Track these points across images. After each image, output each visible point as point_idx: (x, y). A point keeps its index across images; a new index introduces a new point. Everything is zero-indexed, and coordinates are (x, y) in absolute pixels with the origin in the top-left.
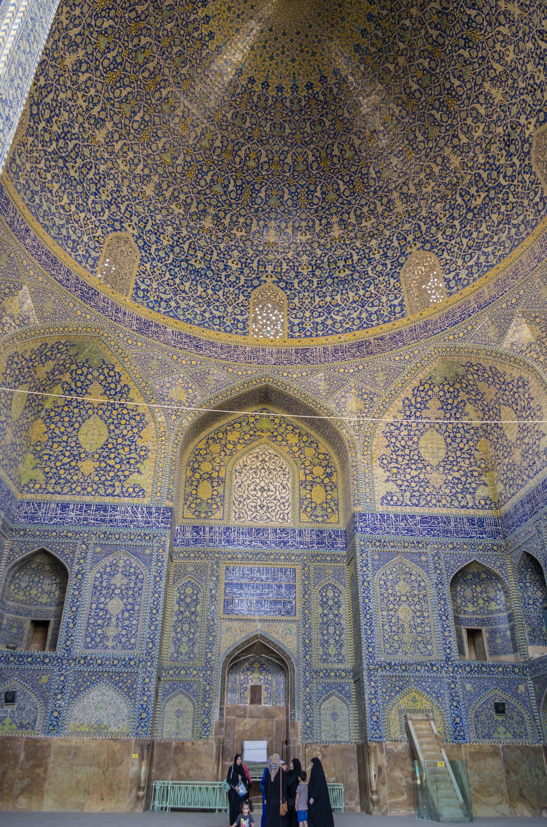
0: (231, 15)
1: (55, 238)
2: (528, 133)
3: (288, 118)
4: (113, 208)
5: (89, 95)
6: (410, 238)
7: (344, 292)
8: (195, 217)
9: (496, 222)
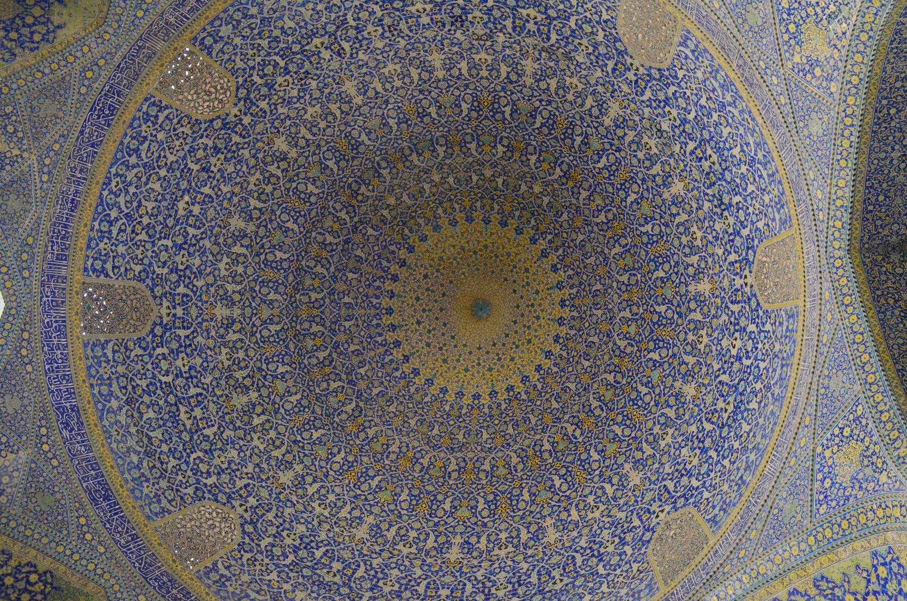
2: (428, 7)
4: (629, 537)
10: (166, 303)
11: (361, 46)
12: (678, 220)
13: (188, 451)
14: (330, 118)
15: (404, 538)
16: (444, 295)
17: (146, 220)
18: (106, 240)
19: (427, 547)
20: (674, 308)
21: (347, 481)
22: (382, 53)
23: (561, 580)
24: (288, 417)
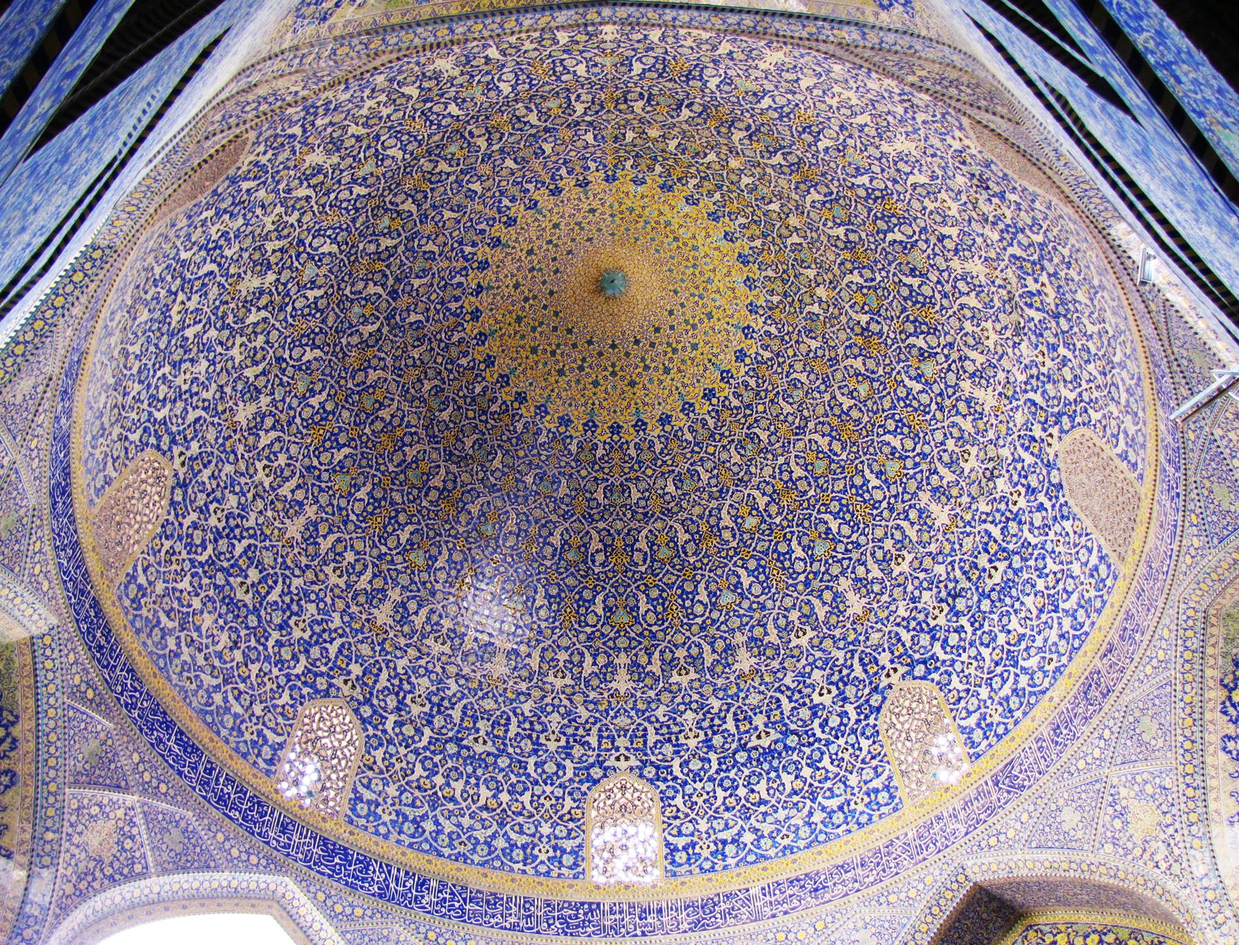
0: (570, 376)
1: (482, 865)
3: (750, 420)
4: (577, 751)
5: (444, 631)
6: (1037, 432)
7: (1017, 605)
8: (719, 669)
16: (590, 240)
23: (485, 742)
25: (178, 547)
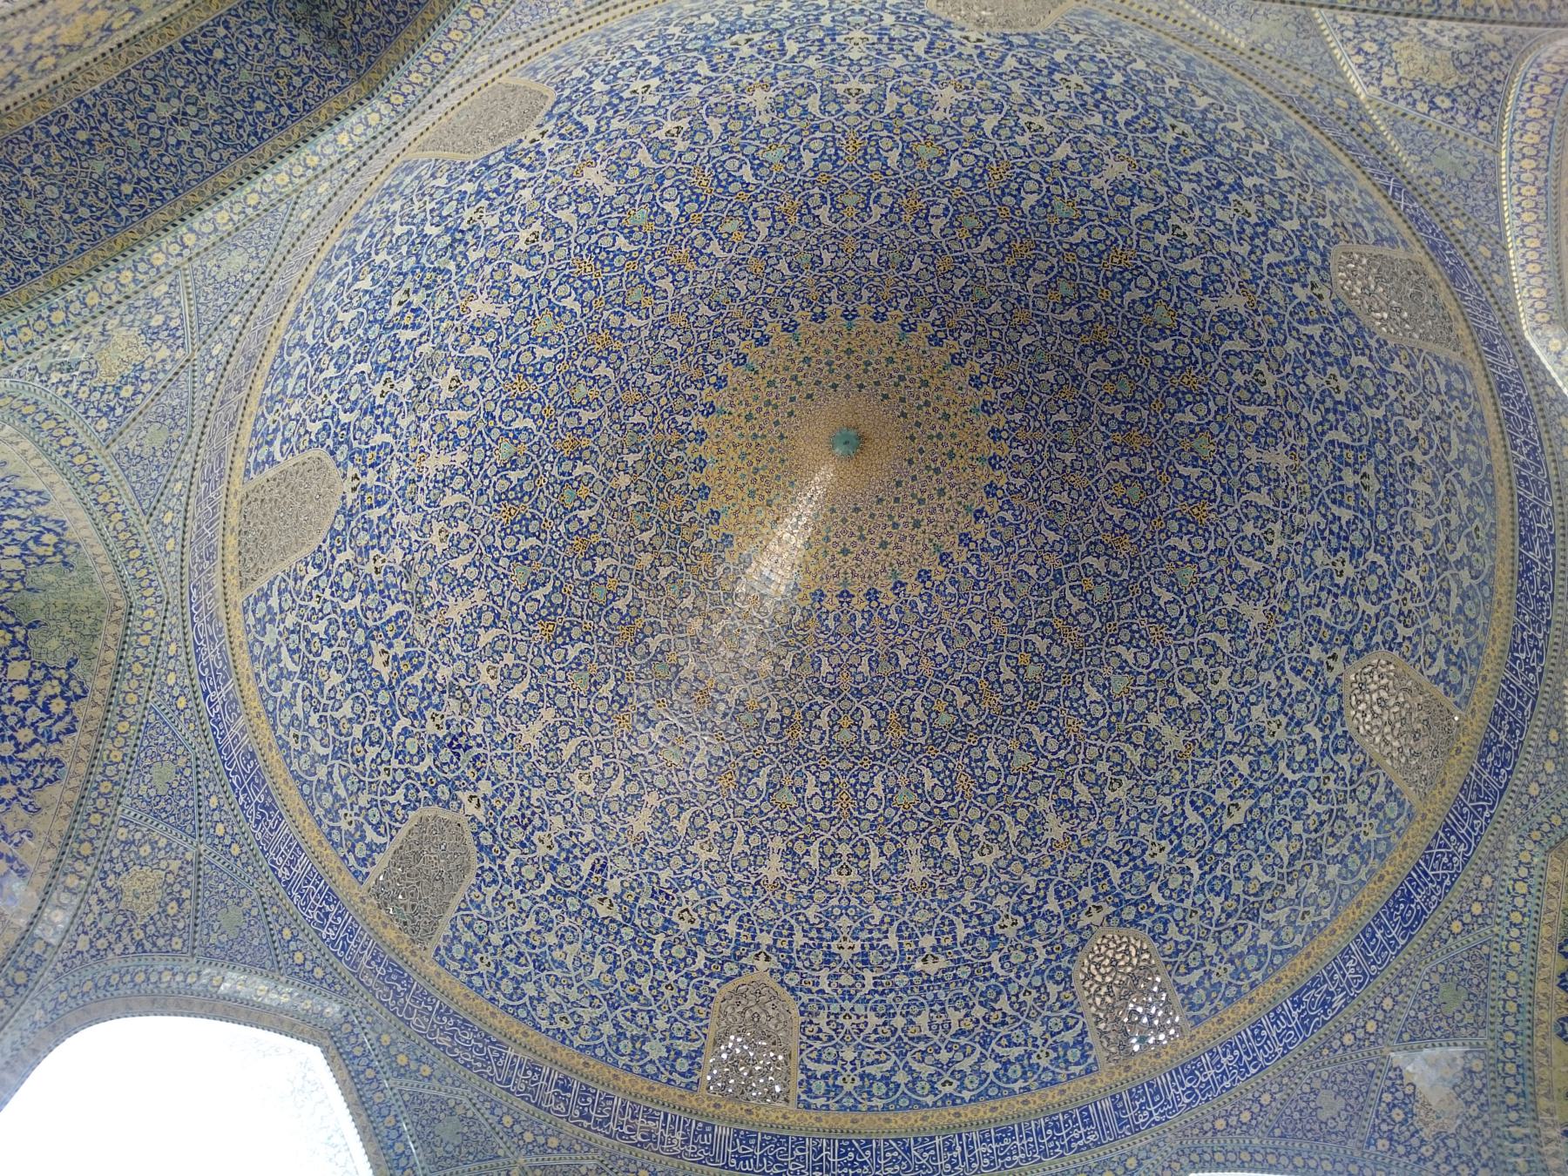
4: (1042, 63)
6: (371, 478)
9: (337, 715)
10: (1084, 921)
11: (575, 846)
12: (526, 274)
13: (1286, 787)
14: (699, 822)
15: (1253, 389)
16: (857, 510)
17: (979, 1012)
18: (1034, 1060)
19: (1247, 347)
20: (658, 194)
21: (1212, 515)
22: (567, 811)
23: (1173, 127)
24: (1161, 651)
25: (1394, 610)
